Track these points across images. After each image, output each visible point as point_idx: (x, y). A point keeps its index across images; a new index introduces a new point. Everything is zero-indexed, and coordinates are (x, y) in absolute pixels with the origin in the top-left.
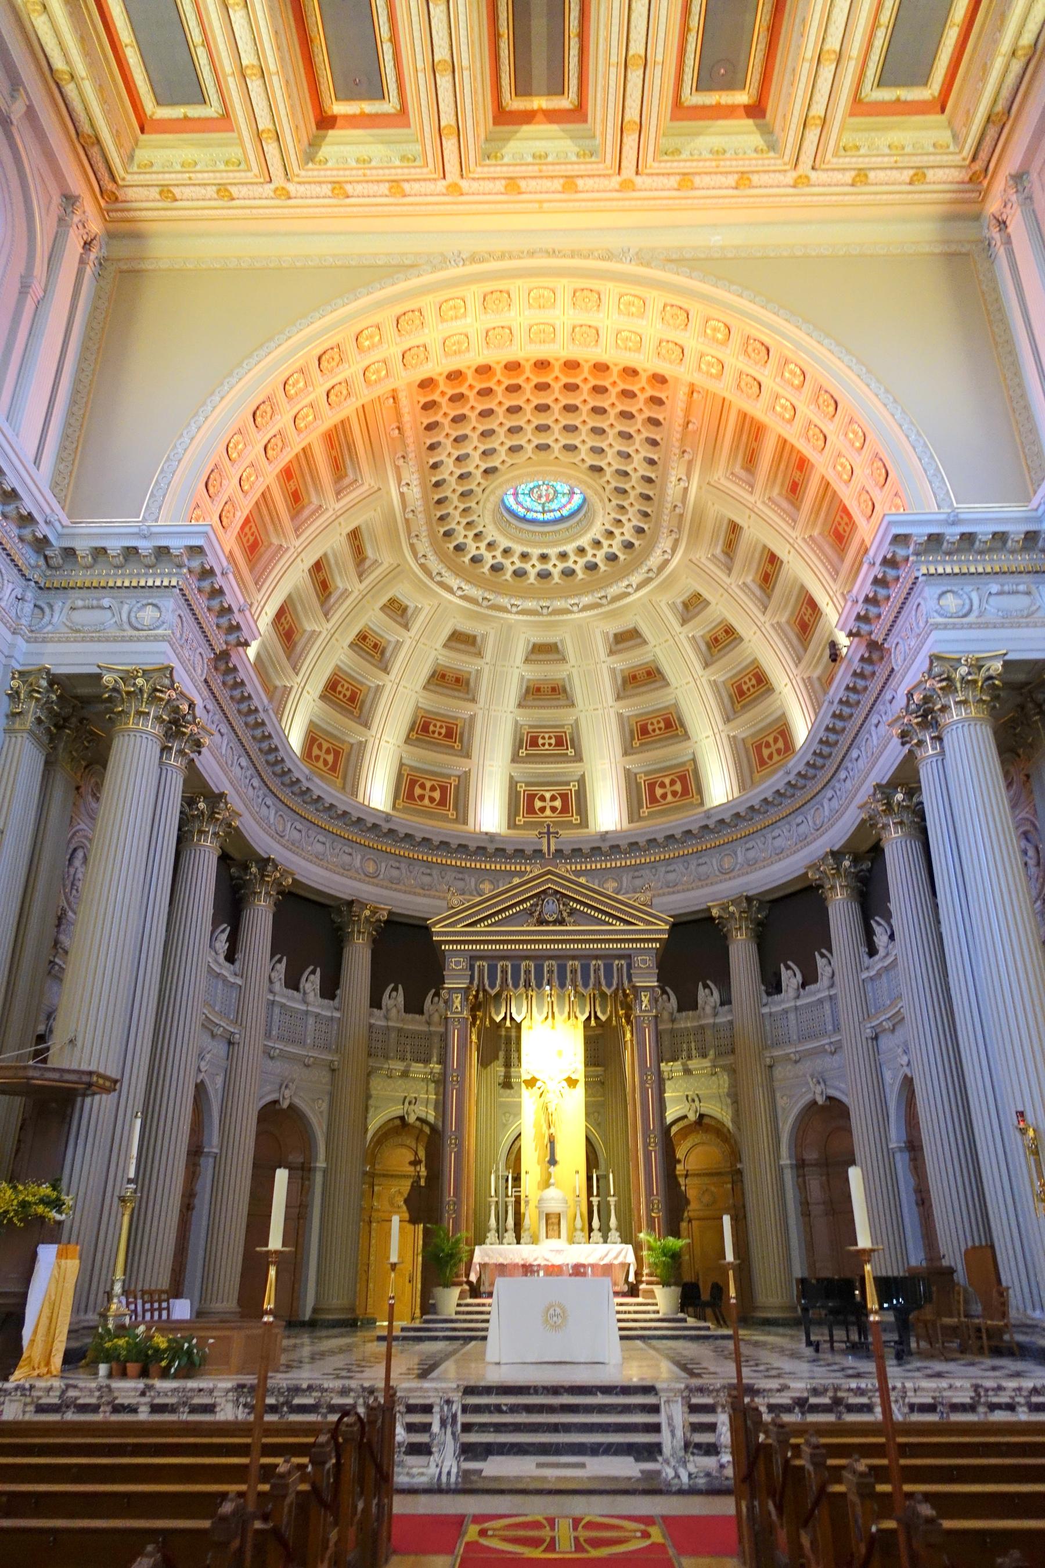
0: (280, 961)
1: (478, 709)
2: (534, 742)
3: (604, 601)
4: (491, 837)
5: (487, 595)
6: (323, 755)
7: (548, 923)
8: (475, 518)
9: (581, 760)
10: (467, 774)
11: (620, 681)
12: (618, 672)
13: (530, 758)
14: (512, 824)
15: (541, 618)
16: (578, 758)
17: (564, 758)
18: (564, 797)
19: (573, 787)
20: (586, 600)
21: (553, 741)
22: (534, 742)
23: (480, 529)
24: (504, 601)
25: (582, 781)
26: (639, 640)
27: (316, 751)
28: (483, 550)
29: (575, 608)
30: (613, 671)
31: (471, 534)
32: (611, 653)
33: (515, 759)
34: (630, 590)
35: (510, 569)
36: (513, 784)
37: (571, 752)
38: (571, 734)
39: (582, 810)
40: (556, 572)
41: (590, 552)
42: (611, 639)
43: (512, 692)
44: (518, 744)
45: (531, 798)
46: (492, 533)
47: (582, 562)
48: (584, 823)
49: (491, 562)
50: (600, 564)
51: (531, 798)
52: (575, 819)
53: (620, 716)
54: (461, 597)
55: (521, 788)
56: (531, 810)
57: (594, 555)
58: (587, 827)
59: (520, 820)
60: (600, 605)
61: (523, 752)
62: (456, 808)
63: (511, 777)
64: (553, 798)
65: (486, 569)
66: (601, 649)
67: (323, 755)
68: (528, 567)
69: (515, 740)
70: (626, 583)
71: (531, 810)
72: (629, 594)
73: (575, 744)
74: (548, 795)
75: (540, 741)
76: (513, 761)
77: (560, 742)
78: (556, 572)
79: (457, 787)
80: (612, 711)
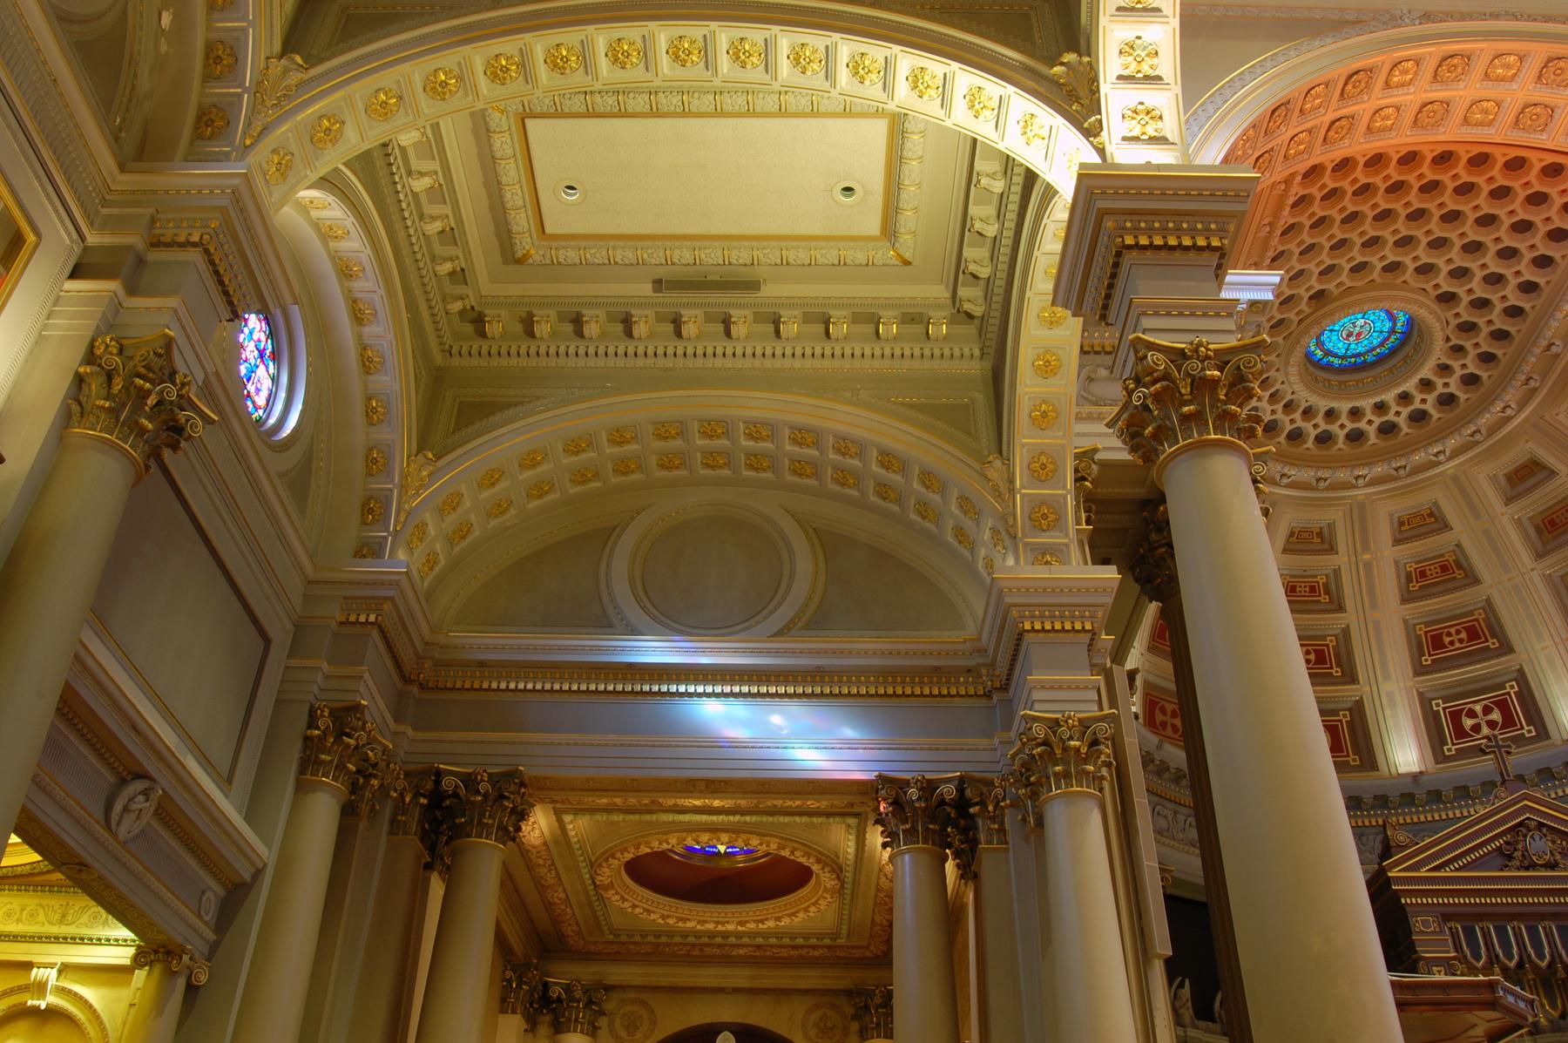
0: (1181, 985)
1: (1350, 618)
2: (1437, 642)
3: (1478, 437)
4: (1416, 777)
5: (1320, 474)
6: (1168, 718)
7: (1533, 866)
8: (1278, 386)
9: (1511, 650)
10: (1359, 705)
11: (1532, 533)
12: (1527, 523)
13: (1438, 666)
14: (1439, 757)
15: (1399, 483)
16: (1506, 648)
17: (1484, 654)
18: (1503, 706)
19: (1512, 689)
20: (1452, 443)
21: (1463, 635)
22: (1437, 642)
23: (1289, 397)
24: (1342, 475)
25: (1521, 678)
26: (1544, 474)
27: (1159, 717)
28: (1300, 423)
29: (1442, 458)
30: (1519, 522)
31: (1279, 407)
32: (1509, 501)
33: (1419, 671)
34: (1509, 412)
35: (1342, 434)
36: (1425, 702)
37: (1493, 643)
38: (1486, 620)
39: (1535, 714)
40: (1401, 421)
41: (1439, 382)
42: (1503, 480)
43: (1389, 585)
44: (1417, 650)
45: (1456, 717)
46: (1306, 397)
47: (1431, 398)
48: (1543, 733)
49: (1313, 433)
50: (1458, 393)
51: (1456, 717)
52: (1528, 731)
53: (1549, 579)
54: (1288, 486)
55: (1439, 706)
56: (1460, 733)
57: (1446, 385)
58: (1548, 737)
59: (1450, 749)
60: (1477, 443)
61: (1427, 660)
62: (1356, 751)
63: (1420, 694)
64: (1487, 710)
65: (1310, 443)
66: (1492, 497)
67: (1168, 718)
68: (1363, 425)
69: (1410, 646)
70: (1499, 406)
71: (1460, 733)
72: (1509, 419)
73: (1497, 630)
74: (1478, 708)
75: (1447, 640)
76: (1417, 673)
77: (1473, 634)
78: (1401, 421)
79: (1351, 724)
80: (1535, 576)
